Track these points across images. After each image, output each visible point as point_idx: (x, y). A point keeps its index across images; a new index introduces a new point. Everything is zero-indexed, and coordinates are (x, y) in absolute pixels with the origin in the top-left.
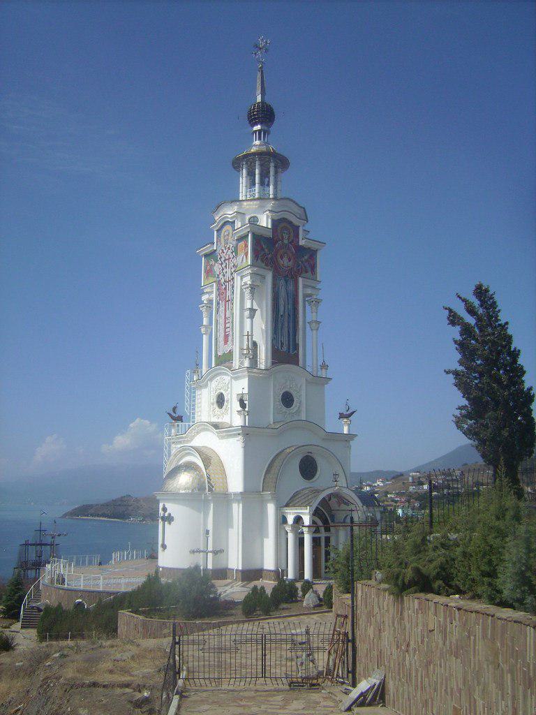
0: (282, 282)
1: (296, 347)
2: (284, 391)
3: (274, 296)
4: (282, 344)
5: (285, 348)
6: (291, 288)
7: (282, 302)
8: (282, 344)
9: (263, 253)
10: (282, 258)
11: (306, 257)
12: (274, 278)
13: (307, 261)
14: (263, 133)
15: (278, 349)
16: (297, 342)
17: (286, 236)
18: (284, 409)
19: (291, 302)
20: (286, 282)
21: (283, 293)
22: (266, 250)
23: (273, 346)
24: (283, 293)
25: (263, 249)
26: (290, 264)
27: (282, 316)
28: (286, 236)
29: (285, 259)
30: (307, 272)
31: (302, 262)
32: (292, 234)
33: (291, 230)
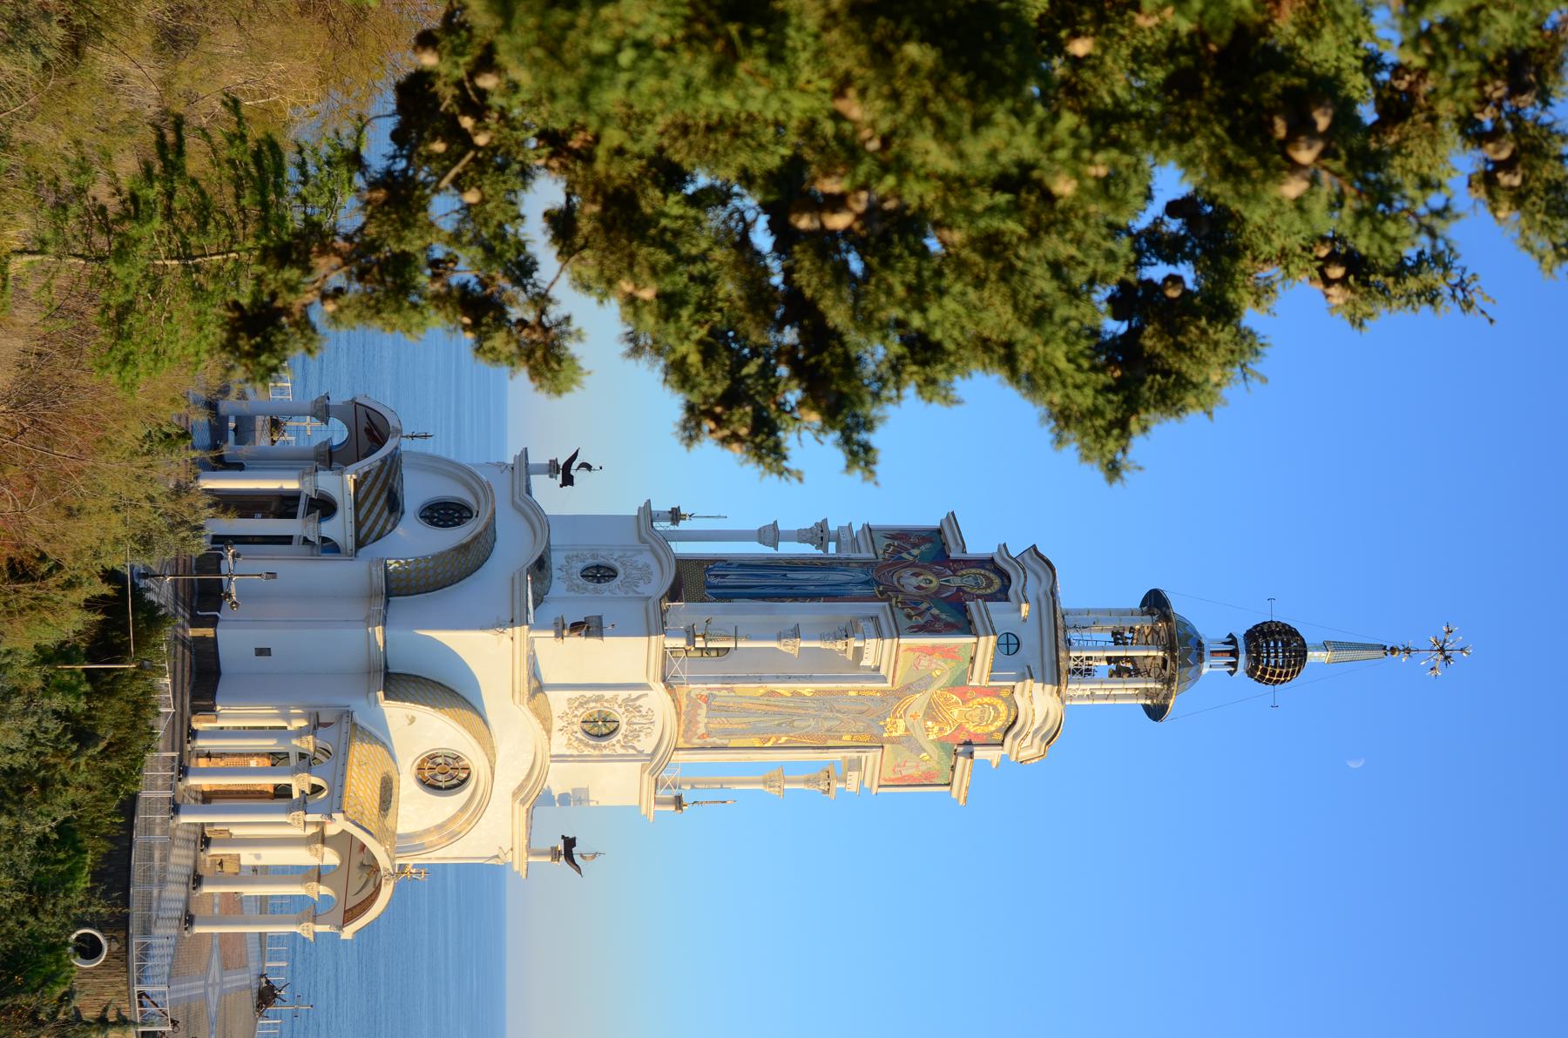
0: (863, 577)
2: (617, 565)
4: (723, 576)
6: (857, 591)
7: (816, 575)
8: (723, 576)
10: (916, 575)
11: (943, 616)
12: (865, 565)
14: (1231, 648)
15: (708, 570)
18: (579, 566)
19: (827, 590)
20: (866, 583)
25: (915, 546)
28: (971, 581)
29: (914, 581)
31: (928, 609)
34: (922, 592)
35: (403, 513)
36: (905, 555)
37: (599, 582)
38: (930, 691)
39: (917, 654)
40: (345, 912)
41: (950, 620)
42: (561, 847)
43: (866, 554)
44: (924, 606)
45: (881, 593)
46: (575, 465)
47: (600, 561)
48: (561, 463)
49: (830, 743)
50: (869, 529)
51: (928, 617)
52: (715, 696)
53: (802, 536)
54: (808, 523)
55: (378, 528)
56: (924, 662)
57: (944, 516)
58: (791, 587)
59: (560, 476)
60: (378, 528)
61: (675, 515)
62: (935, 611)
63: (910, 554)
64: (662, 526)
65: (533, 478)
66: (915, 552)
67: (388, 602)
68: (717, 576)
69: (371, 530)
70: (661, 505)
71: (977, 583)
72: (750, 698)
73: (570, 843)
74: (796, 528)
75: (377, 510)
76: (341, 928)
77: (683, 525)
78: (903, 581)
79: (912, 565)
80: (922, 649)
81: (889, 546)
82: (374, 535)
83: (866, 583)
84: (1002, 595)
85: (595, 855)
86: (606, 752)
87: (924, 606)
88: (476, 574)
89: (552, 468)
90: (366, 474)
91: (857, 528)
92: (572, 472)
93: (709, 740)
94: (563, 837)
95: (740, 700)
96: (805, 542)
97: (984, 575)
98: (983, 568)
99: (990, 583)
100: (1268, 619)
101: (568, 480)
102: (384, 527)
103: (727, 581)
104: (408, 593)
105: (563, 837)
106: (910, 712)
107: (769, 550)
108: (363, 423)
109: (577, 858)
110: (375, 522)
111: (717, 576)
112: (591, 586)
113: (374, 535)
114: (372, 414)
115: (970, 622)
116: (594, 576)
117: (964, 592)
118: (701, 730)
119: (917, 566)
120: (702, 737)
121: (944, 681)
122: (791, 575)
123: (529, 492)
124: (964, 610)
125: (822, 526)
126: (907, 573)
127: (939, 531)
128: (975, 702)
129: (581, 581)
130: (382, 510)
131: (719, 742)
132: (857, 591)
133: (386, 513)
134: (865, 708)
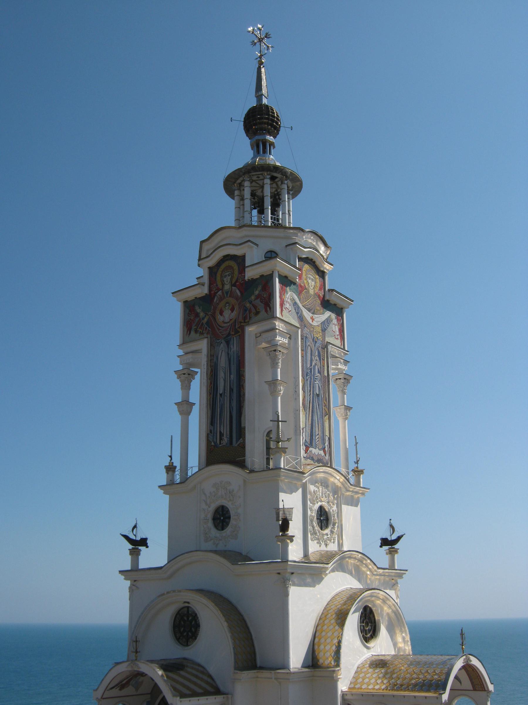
0: (223, 345)
1: (241, 432)
3: (212, 371)
4: (221, 435)
5: (226, 440)
7: (221, 375)
8: (221, 435)
9: (197, 320)
10: (221, 313)
11: (257, 292)
12: (212, 346)
13: (257, 297)
15: (216, 446)
16: (242, 426)
17: (227, 280)
18: (214, 532)
19: (234, 368)
20: (228, 343)
21: (223, 362)
22: (202, 315)
23: (208, 442)
24: (223, 362)
25: (197, 315)
26: (234, 314)
27: (221, 395)
28: (227, 280)
30: (257, 313)
31: (251, 302)
32: (236, 272)
33: (236, 267)
34: (236, 308)
35: (185, 659)
36: (206, 320)
37: (229, 518)
38: (300, 305)
39: (284, 309)
40: (475, 689)
41: (260, 288)
42: (386, 548)
43: (203, 345)
44: (248, 305)
45: (237, 332)
46: (132, 537)
47: (210, 516)
48: (131, 547)
49: (326, 374)
50: (184, 343)
51: (258, 302)
52: (306, 440)
53: (186, 387)
54: (178, 383)
55: (205, 678)
56: (287, 306)
57: (175, 299)
58: (231, 390)
59: (140, 548)
60: (205, 678)
61: (170, 469)
62: (253, 297)
63: (203, 319)
64: (178, 478)
65: (141, 566)
66: (202, 315)
67: (261, 668)
68: (221, 439)
69: (207, 683)
70: (163, 479)
71: (229, 275)
72: (306, 419)
73: (385, 542)
74: (180, 392)
75: (181, 680)
76: (489, 692)
77: (177, 462)
78: (227, 320)
79: (214, 316)
80: (282, 305)
81: (196, 332)
82: (209, 680)
83: (228, 343)
84: (240, 260)
85: (391, 526)
86: (336, 515)
87: (248, 305)
88: (234, 602)
89: (135, 553)
90: (175, 689)
91: (181, 352)
92: (138, 538)
93: (326, 449)
94: (381, 546)
95: (307, 428)
96: (190, 386)
97: (222, 271)
98: (216, 274)
99: (230, 267)
100: (242, 124)
101: (144, 542)
102: (202, 673)
103: (226, 431)
104: (254, 653)
105: (381, 546)
106: (310, 321)
107: (196, 410)
108: (116, 692)
109: (394, 537)
110: (202, 680)
111: (221, 439)
112: (232, 522)
113: (209, 680)
114: (111, 686)
115: (262, 276)
116: (223, 521)
117: (237, 281)
118: (322, 452)
119: (214, 313)
120: (325, 452)
121: (296, 297)
122: (221, 390)
123: (161, 568)
124: (253, 282)
125: (180, 374)
126: (220, 318)
127: (186, 303)
128: (305, 281)
129: (228, 530)
130: (180, 675)
131: (327, 443)
132: (235, 348)
133: (182, 673)
134: (309, 348)
